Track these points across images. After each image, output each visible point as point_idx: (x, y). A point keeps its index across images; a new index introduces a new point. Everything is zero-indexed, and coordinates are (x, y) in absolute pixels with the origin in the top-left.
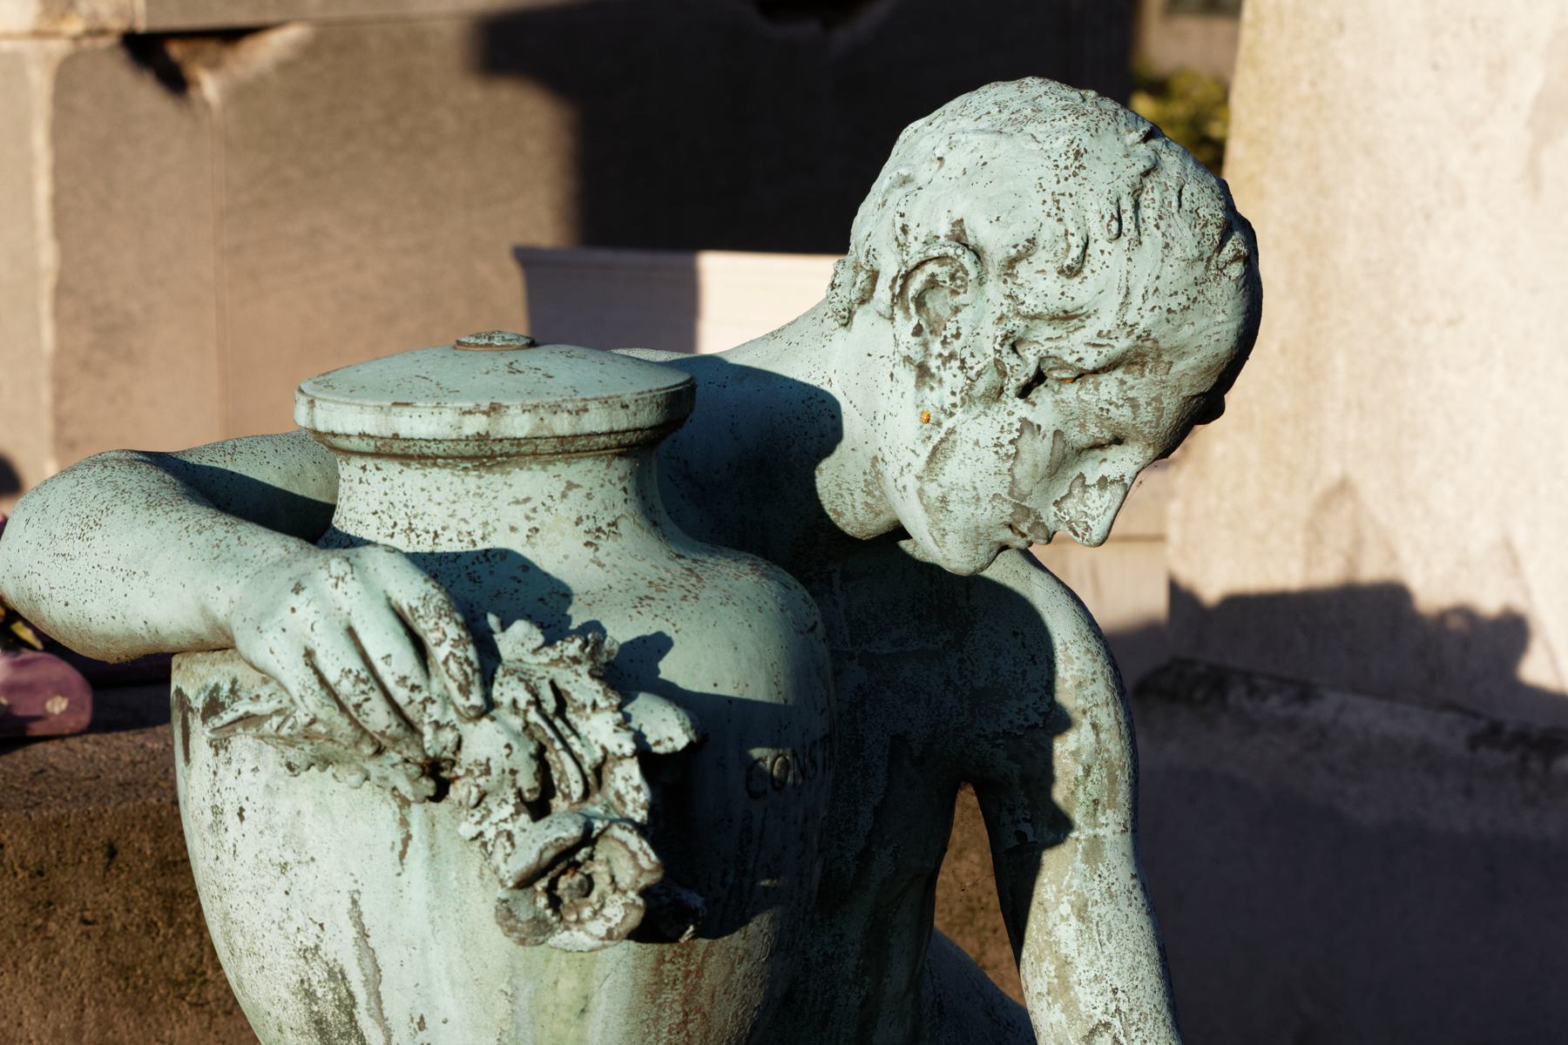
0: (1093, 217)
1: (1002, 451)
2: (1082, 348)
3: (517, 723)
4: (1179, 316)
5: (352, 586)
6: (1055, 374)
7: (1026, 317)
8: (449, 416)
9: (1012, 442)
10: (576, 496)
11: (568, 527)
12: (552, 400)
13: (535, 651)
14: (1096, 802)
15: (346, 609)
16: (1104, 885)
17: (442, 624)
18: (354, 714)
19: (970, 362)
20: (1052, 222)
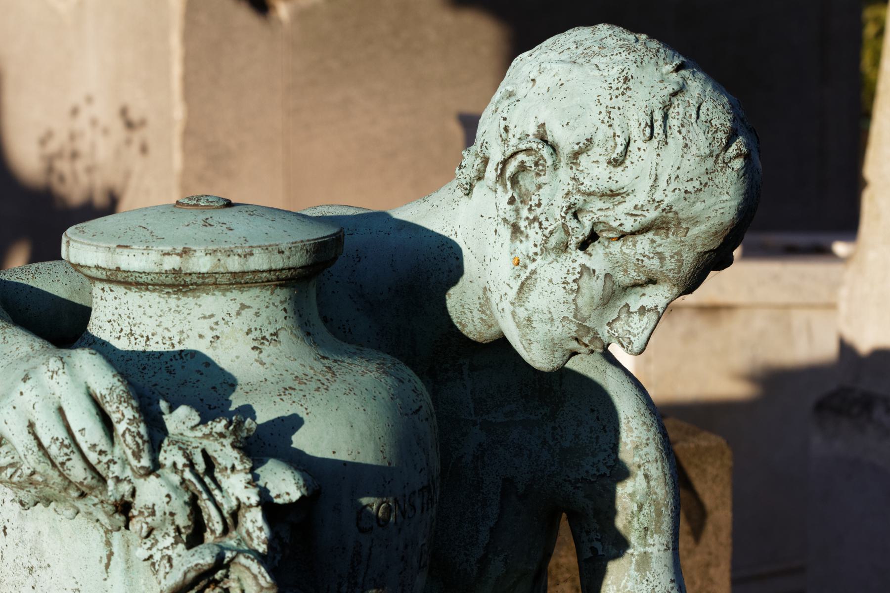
0: (633, 124)
1: (568, 287)
2: (623, 217)
3: (176, 479)
4: (693, 195)
5: (62, 378)
6: (604, 234)
7: (584, 194)
8: (154, 256)
9: (575, 281)
10: (248, 314)
11: (241, 336)
12: (227, 247)
13: (193, 428)
14: (646, 529)
15: (58, 394)
16: (650, 587)
17: (122, 408)
18: (61, 469)
19: (545, 224)
20: (604, 127)
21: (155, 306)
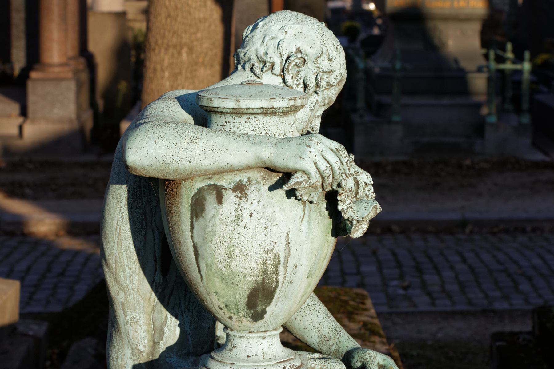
8: (286, 101)
18: (326, 178)
20: (324, 47)
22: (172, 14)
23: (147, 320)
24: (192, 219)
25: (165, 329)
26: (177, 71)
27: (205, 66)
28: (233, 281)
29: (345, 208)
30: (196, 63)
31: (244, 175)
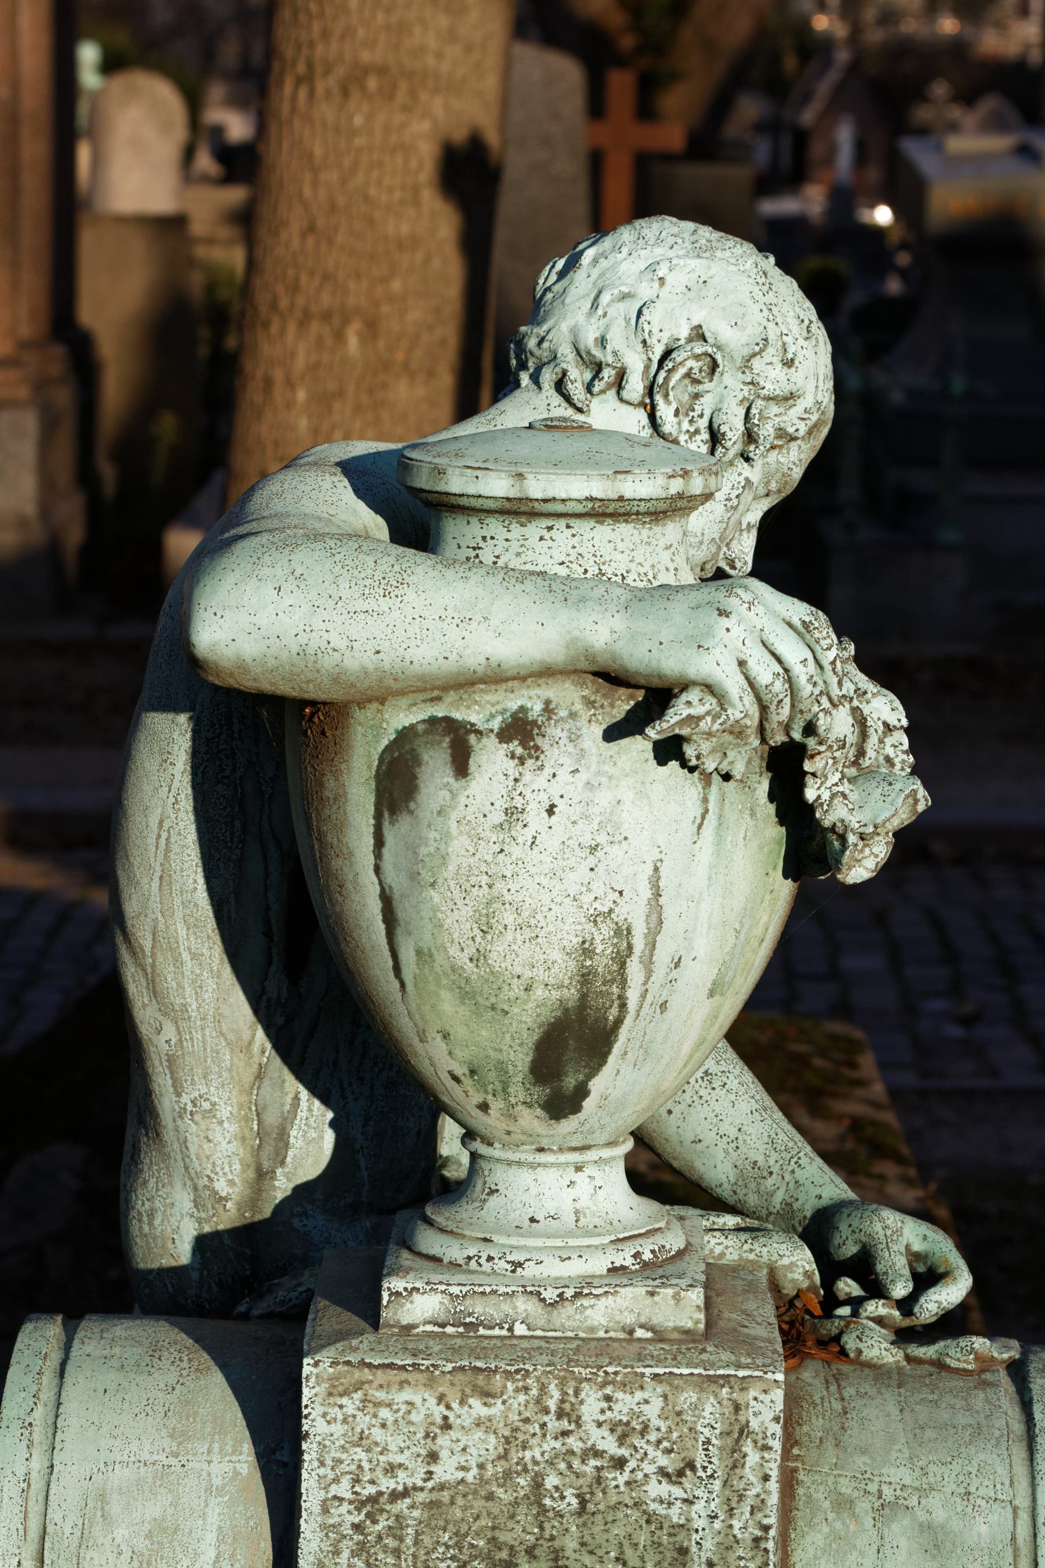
1: (729, 504)
8: (661, 480)
15: (759, 627)
18: (773, 707)
20: (771, 326)
21: (627, 540)
22: (321, 223)
23: (241, 1106)
24: (378, 817)
25: (293, 1133)
26: (332, 386)
27: (412, 375)
28: (493, 1000)
29: (826, 796)
30: (387, 366)
31: (533, 692)
